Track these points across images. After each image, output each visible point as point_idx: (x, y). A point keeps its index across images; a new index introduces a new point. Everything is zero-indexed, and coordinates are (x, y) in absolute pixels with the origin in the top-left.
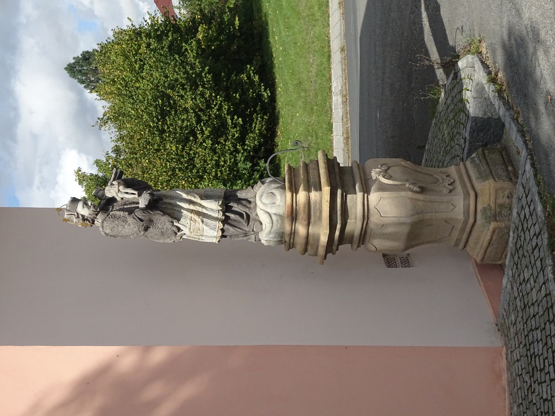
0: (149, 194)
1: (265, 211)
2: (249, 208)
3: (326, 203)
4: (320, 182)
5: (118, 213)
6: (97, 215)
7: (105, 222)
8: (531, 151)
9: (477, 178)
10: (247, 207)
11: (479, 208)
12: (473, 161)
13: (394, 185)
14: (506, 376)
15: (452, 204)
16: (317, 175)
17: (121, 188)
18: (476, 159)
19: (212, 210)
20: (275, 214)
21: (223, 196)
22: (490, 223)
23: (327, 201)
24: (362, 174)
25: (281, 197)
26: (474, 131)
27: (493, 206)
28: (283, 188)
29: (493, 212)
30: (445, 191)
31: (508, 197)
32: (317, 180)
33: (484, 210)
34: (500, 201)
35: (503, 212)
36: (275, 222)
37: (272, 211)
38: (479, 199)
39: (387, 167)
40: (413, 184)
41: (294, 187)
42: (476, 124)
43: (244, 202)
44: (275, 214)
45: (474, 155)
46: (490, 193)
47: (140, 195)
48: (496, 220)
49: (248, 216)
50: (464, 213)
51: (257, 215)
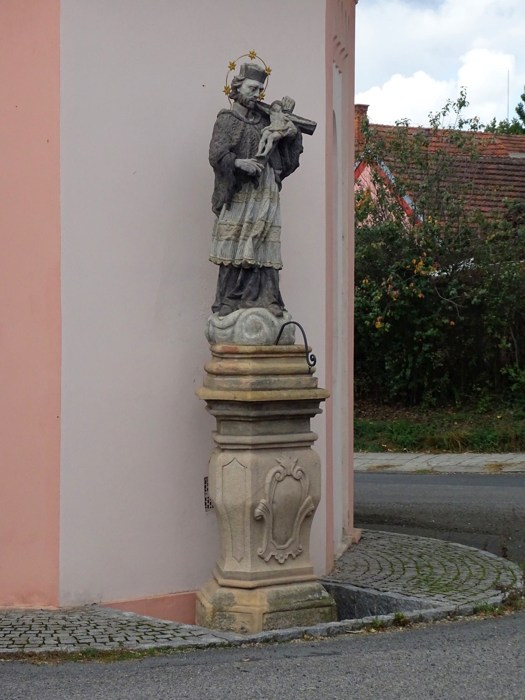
0: (257, 171)
1: (237, 318)
2: (245, 299)
3: (233, 396)
4: (271, 390)
5: (239, 132)
6: (242, 104)
7: (229, 115)
8: (236, 646)
9: (277, 593)
10: (247, 296)
11: (234, 592)
12: (313, 591)
13: (264, 485)
14: (22, 608)
15: (242, 559)
16: (286, 386)
17: (276, 135)
19: (242, 251)
20: (233, 332)
21: (265, 265)
22: (212, 603)
23: (235, 398)
24: (293, 445)
25: (255, 340)
26: (388, 602)
27: (234, 608)
28: (267, 344)
29: (225, 608)
30: (260, 549)
31: (242, 628)
32: (275, 386)
33: (231, 598)
34: (238, 618)
35: (225, 620)
36: (224, 332)
37: (237, 329)
38: (245, 593)
39: (298, 478)
40: (266, 509)
41: (265, 356)
42: (394, 605)
43: (255, 293)
44: (233, 332)
45: (325, 594)
46: (249, 606)
47: (260, 158)
48: (214, 611)
49: (239, 298)
50: (231, 572)
51: (238, 309)
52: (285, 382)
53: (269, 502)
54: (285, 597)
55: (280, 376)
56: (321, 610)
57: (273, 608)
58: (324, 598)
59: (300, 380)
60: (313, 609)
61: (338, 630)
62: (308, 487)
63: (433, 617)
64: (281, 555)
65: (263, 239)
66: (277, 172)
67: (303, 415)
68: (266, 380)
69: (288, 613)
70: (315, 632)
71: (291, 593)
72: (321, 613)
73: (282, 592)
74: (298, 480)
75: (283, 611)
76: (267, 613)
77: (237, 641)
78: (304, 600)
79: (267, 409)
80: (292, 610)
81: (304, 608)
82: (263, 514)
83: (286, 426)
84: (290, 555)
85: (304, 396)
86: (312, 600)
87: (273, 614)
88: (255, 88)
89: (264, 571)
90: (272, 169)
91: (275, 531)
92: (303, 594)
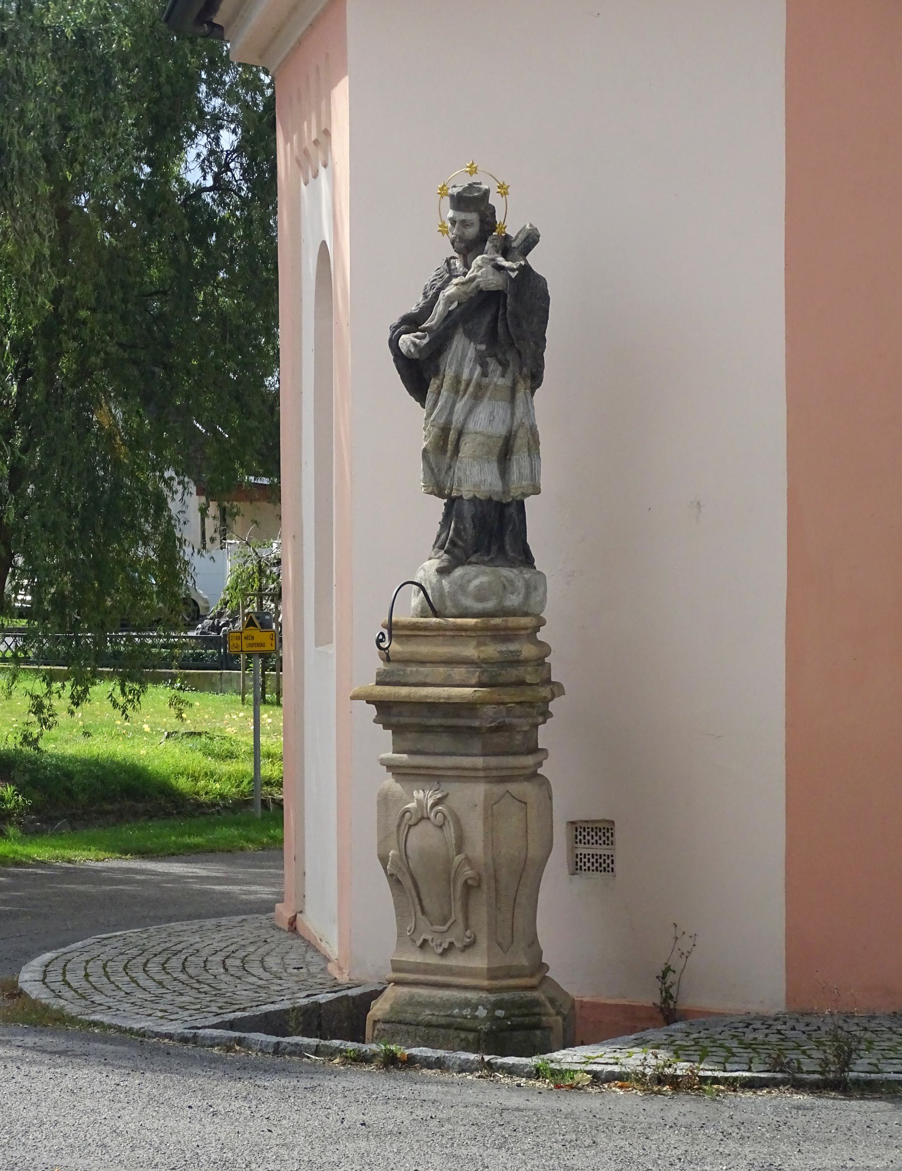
9: (412, 997)
12: (467, 1004)
16: (428, 680)
32: (412, 680)
41: (408, 633)
43: (443, 536)
52: (427, 676)
53: (401, 855)
54: (419, 1004)
55: (428, 665)
57: (388, 1017)
59: (451, 672)
60: (451, 1032)
61: (293, 1048)
62: (454, 842)
64: (438, 942)
65: (449, 454)
68: (398, 670)
70: (255, 1044)
71: (432, 999)
72: (462, 1040)
73: (420, 996)
74: (441, 827)
75: (406, 1024)
76: (379, 1021)
77: (152, 1031)
78: (442, 1013)
79: (400, 714)
80: (418, 1025)
81: (439, 1026)
82: (395, 872)
83: (444, 742)
84: (451, 944)
85: (430, 697)
86: (454, 1017)
88: (453, 222)
90: (472, 344)
91: (425, 903)
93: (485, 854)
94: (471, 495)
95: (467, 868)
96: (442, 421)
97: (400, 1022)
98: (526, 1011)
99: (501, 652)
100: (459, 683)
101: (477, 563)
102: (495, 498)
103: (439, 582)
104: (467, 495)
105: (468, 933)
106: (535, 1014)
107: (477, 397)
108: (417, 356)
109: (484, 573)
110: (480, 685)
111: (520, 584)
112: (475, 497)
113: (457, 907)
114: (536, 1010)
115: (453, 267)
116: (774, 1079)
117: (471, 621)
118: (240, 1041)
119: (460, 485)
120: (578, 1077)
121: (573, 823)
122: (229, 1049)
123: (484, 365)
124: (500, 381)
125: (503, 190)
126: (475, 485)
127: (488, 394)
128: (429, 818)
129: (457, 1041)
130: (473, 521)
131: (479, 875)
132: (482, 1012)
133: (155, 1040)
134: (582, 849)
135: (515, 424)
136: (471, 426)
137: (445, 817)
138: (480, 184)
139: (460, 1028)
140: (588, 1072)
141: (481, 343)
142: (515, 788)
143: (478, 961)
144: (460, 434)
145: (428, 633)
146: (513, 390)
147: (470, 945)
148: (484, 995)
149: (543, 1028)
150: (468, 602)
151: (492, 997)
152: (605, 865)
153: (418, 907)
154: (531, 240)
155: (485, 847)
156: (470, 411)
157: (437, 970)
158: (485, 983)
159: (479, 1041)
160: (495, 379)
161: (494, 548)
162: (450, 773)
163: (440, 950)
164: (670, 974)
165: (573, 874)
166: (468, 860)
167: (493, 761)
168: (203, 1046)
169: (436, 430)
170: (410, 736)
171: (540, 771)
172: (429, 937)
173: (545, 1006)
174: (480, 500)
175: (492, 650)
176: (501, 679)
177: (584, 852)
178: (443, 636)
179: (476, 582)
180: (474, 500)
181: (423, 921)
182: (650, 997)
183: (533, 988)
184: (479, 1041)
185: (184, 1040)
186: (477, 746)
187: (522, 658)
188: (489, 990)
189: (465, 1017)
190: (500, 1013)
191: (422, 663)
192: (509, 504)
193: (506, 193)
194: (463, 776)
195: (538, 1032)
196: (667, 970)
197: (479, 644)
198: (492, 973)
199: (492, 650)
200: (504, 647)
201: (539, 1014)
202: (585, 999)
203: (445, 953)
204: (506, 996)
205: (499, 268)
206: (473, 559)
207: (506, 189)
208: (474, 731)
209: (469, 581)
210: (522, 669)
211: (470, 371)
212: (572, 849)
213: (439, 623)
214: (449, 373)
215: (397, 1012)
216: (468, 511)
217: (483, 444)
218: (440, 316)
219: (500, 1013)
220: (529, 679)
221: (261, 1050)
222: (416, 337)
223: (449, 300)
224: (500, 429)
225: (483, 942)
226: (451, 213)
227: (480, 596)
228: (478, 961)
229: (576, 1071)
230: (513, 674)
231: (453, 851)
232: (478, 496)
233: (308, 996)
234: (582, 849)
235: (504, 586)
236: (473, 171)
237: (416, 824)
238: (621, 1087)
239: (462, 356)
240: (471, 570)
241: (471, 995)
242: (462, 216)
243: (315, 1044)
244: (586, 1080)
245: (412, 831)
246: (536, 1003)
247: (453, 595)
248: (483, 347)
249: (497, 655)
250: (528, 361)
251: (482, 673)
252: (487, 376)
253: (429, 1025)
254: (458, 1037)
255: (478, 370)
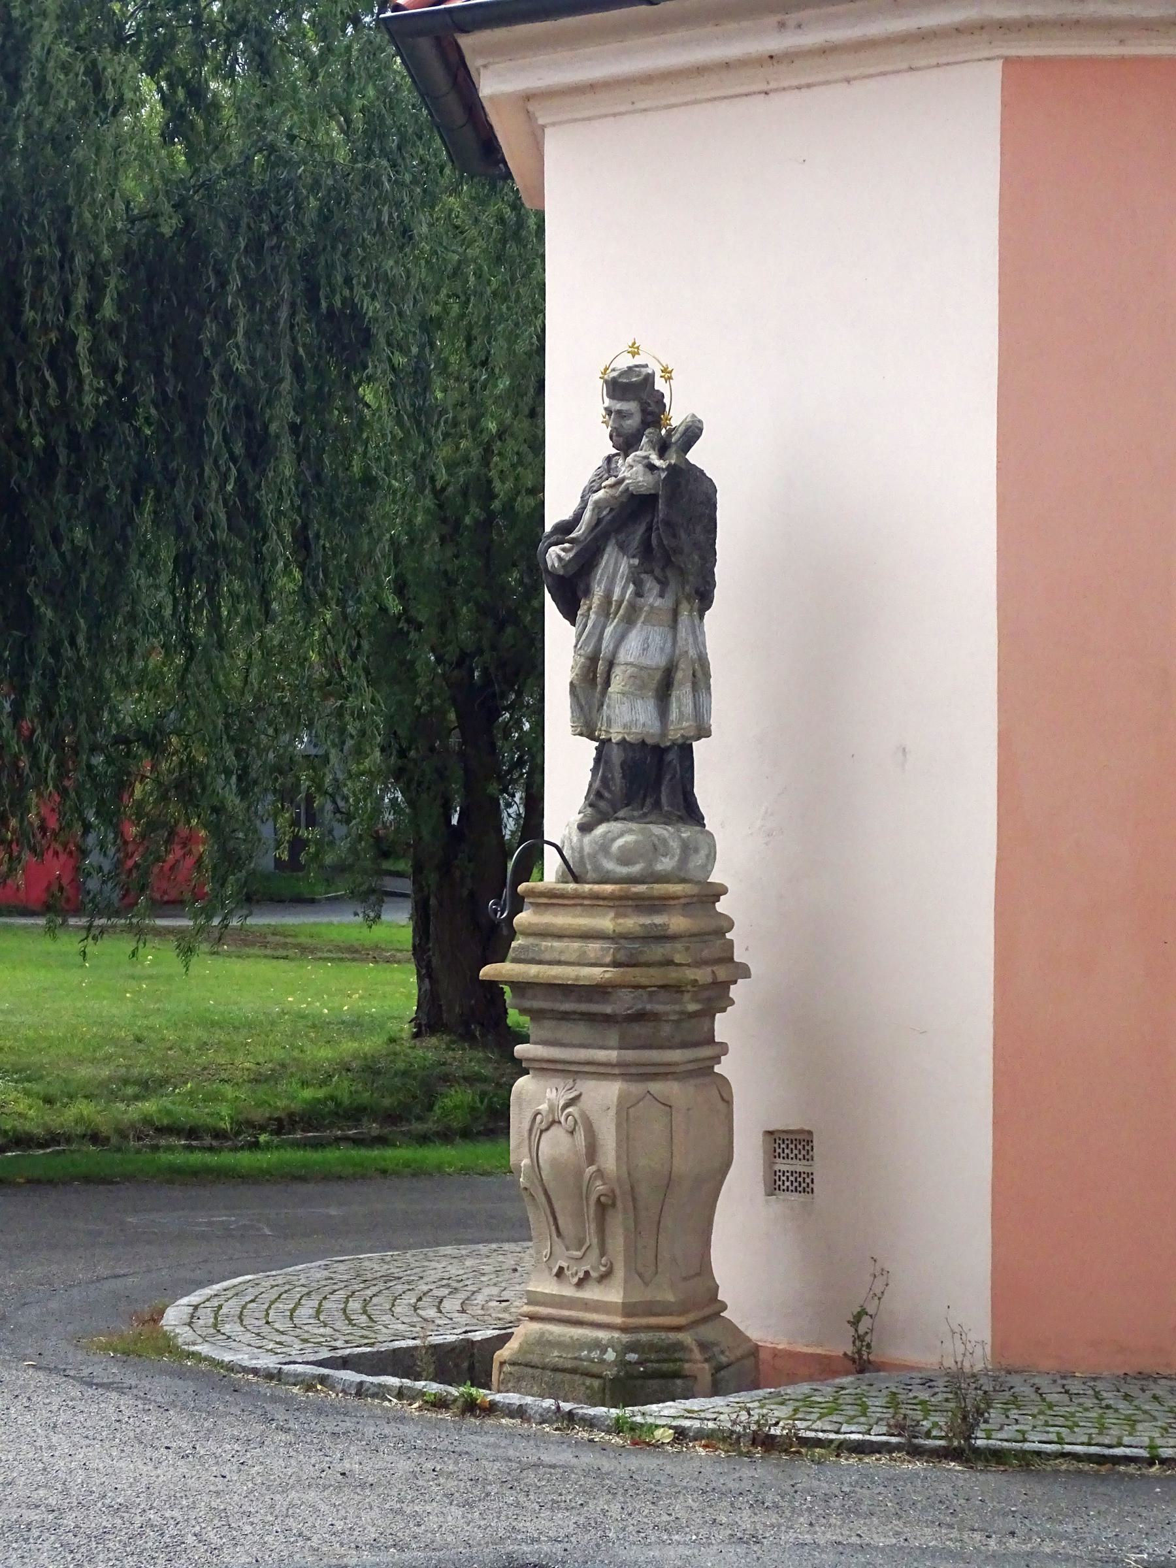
4: (540, 962)
12: (597, 1345)
18: (595, 1354)
32: (547, 956)
52: (561, 952)
53: (533, 1166)
55: (565, 940)
56: (588, 1381)
58: (602, 1361)
60: (577, 1377)
61: (376, 1390)
63: (541, 1415)
66: (632, 561)
67: (595, 1014)
69: (537, 1372)
72: (587, 1388)
73: (551, 1333)
74: (572, 1133)
75: (532, 1367)
79: (534, 997)
80: (543, 1368)
81: (564, 1370)
82: (528, 1185)
83: (580, 1031)
84: (587, 1273)
86: (581, 1360)
87: (516, 1368)
89: (546, 1291)
91: (560, 1222)
92: (580, 1345)
93: (618, 1166)
94: (619, 737)
95: (599, 1182)
96: (589, 649)
97: (526, 1365)
98: (665, 1356)
99: (643, 925)
100: (593, 961)
101: (624, 819)
102: (649, 741)
103: (581, 841)
104: (616, 738)
105: (603, 1261)
106: (675, 1361)
107: (630, 621)
108: (561, 572)
109: (630, 831)
110: (616, 964)
111: (675, 845)
112: (624, 739)
113: (592, 1227)
114: (677, 1355)
115: (613, 466)
116: (887, 1443)
117: (609, 888)
118: (323, 1379)
119: (609, 725)
120: (658, 1433)
121: (771, 1133)
122: (310, 1387)
123: (638, 584)
124: (658, 602)
125: (667, 374)
126: (625, 726)
127: (642, 619)
128: (560, 1122)
129: (583, 1388)
130: (622, 768)
131: (613, 1191)
132: (610, 1355)
133: (240, 1375)
134: (782, 1165)
135: (677, 652)
136: (622, 656)
137: (576, 1122)
138: (646, 366)
139: (588, 1374)
140: (670, 1427)
141: (634, 557)
142: (656, 1087)
143: (613, 1294)
144: (611, 664)
145: (566, 902)
146: (675, 613)
147: (604, 1277)
148: (616, 1335)
149: (685, 1377)
150: (610, 865)
151: (625, 1338)
152: (803, 1184)
153: (553, 1228)
154: (692, 433)
155: (618, 1158)
156: (621, 639)
157: (571, 1303)
158: (618, 1320)
159: (604, 1389)
160: (651, 600)
161: (649, 801)
162: (587, 1069)
163: (575, 1280)
164: (865, 1318)
165: (772, 1195)
166: (600, 1173)
167: (630, 1055)
168: (285, 1384)
169: (583, 660)
170: (548, 1024)
171: (717, 1069)
172: (565, 1265)
173: (691, 1351)
174: (631, 744)
175: (632, 923)
176: (643, 959)
177: (784, 1168)
178: (581, 905)
179: (620, 842)
180: (623, 742)
181: (559, 1248)
182: (842, 1346)
183: (678, 1329)
184: (604, 1389)
185: (269, 1376)
186: (613, 1036)
187: (670, 932)
188: (624, 1329)
189: (592, 1361)
190: (632, 1357)
191: (559, 936)
192: (668, 749)
193: (670, 378)
194: (601, 1071)
195: (679, 1382)
196: (863, 1313)
197: (617, 916)
198: (628, 1309)
199: (632, 923)
200: (646, 920)
201: (681, 1360)
202: (780, 1347)
203: (580, 1284)
204: (643, 1337)
205: (651, 467)
206: (621, 814)
207: (670, 372)
208: (608, 1019)
209: (614, 840)
210: (668, 946)
211: (622, 591)
212: (769, 1164)
213: (576, 890)
214: (598, 592)
215: (526, 1352)
216: (616, 756)
217: (635, 677)
218: (589, 524)
219: (632, 1357)
220: (678, 958)
221: (343, 1391)
222: (564, 550)
223: (598, 505)
224: (657, 659)
225: (620, 1273)
226: (607, 402)
227: (625, 858)
228: (613, 1294)
229: (657, 1426)
230: (658, 952)
231: (584, 1163)
232: (628, 739)
233: (466, 1332)
234: (782, 1165)
235: (654, 845)
236: (634, 351)
237: (547, 1129)
238: (705, 1446)
239: (615, 571)
240: (615, 826)
241: (602, 1335)
242: (618, 406)
243: (399, 1385)
244: (668, 1436)
245: (544, 1136)
246: (679, 1346)
247: (593, 856)
248: (636, 561)
249: (638, 929)
250: (691, 578)
251: (617, 950)
252: (642, 596)
253: (556, 1369)
254: (584, 1384)
255: (631, 587)
